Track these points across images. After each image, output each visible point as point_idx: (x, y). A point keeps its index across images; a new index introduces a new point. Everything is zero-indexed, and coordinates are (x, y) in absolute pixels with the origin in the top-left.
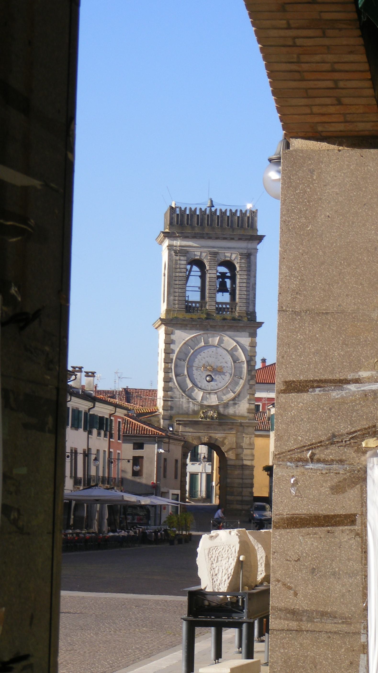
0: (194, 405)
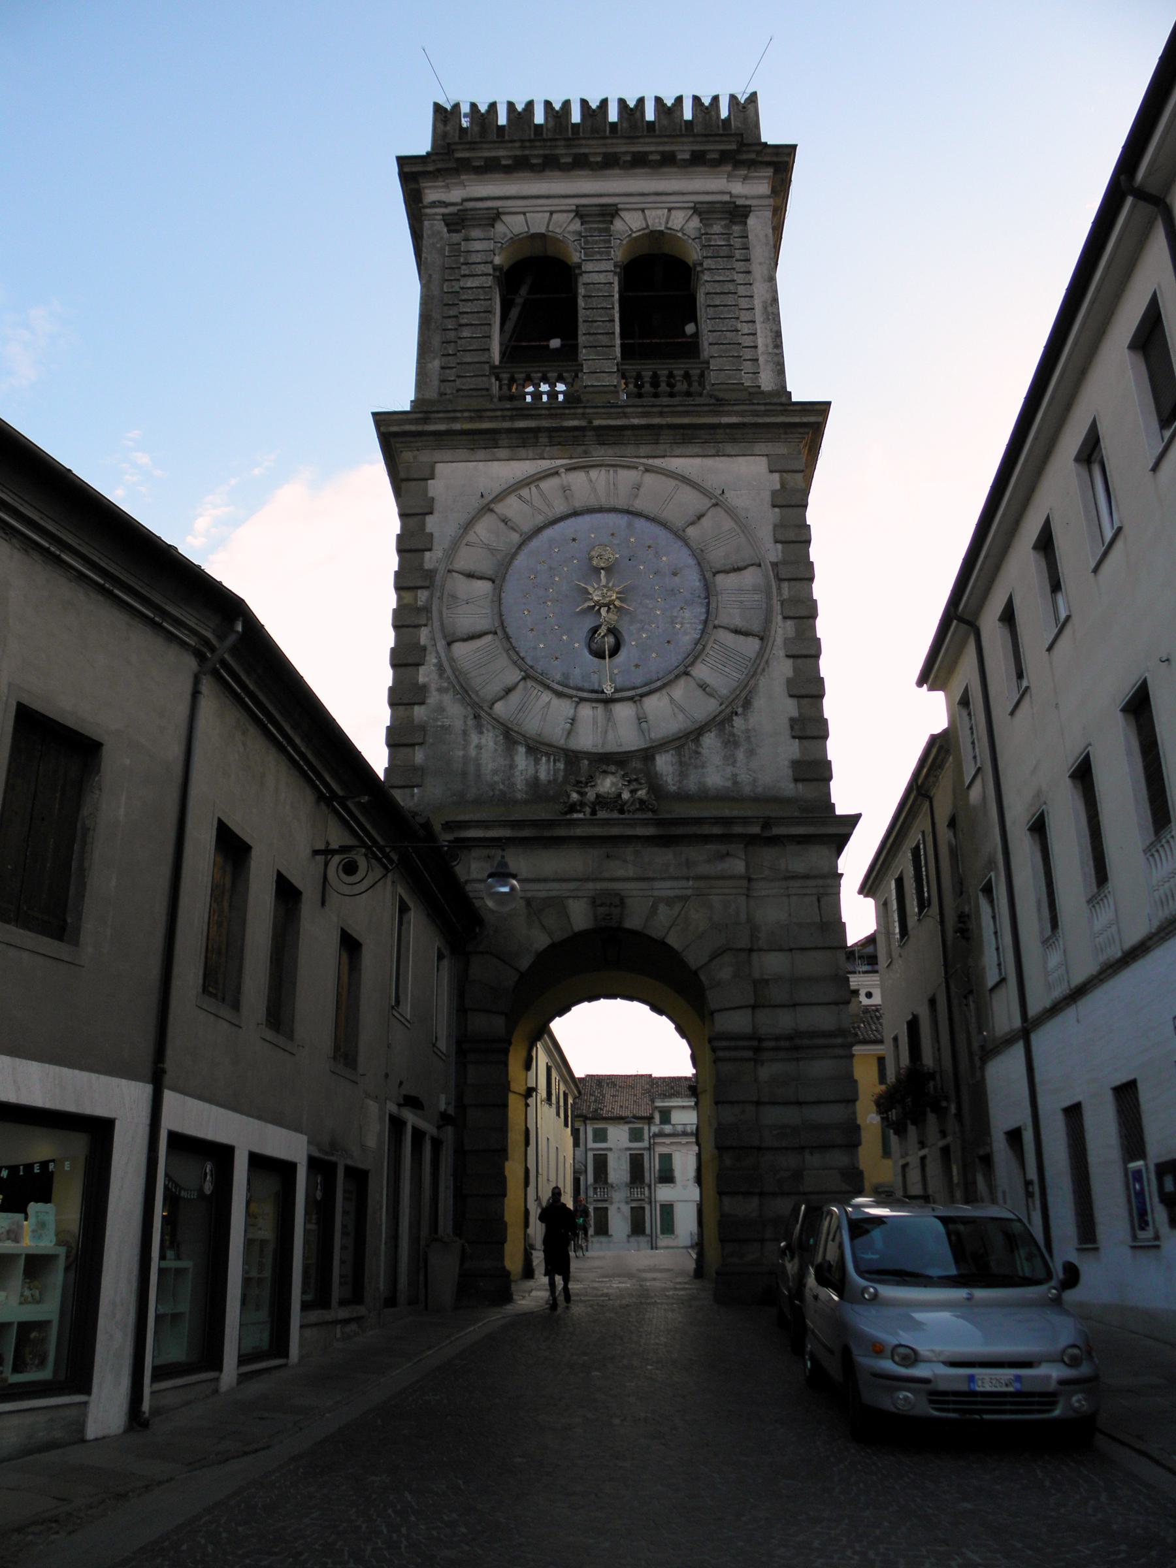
0: (537, 761)
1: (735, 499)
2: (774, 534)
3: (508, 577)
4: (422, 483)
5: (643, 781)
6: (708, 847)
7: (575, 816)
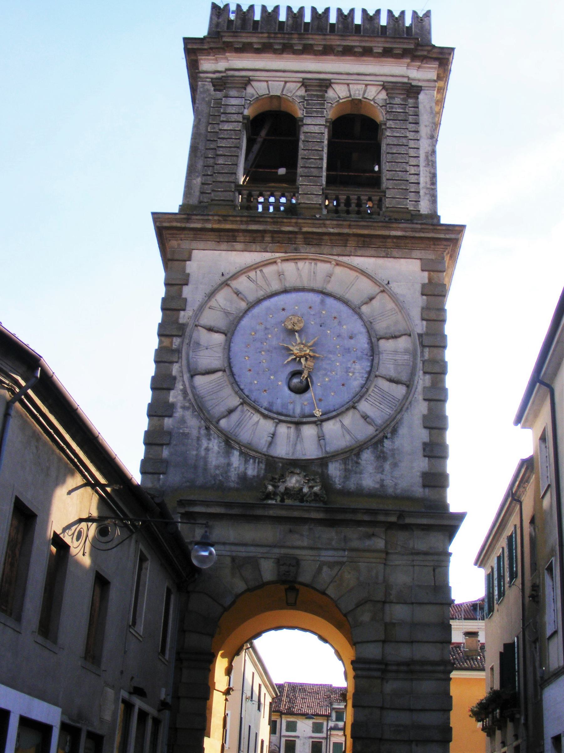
0: (246, 462)
1: (396, 288)
2: (422, 314)
3: (236, 332)
4: (183, 263)
5: (318, 481)
6: (360, 529)
7: (270, 502)
